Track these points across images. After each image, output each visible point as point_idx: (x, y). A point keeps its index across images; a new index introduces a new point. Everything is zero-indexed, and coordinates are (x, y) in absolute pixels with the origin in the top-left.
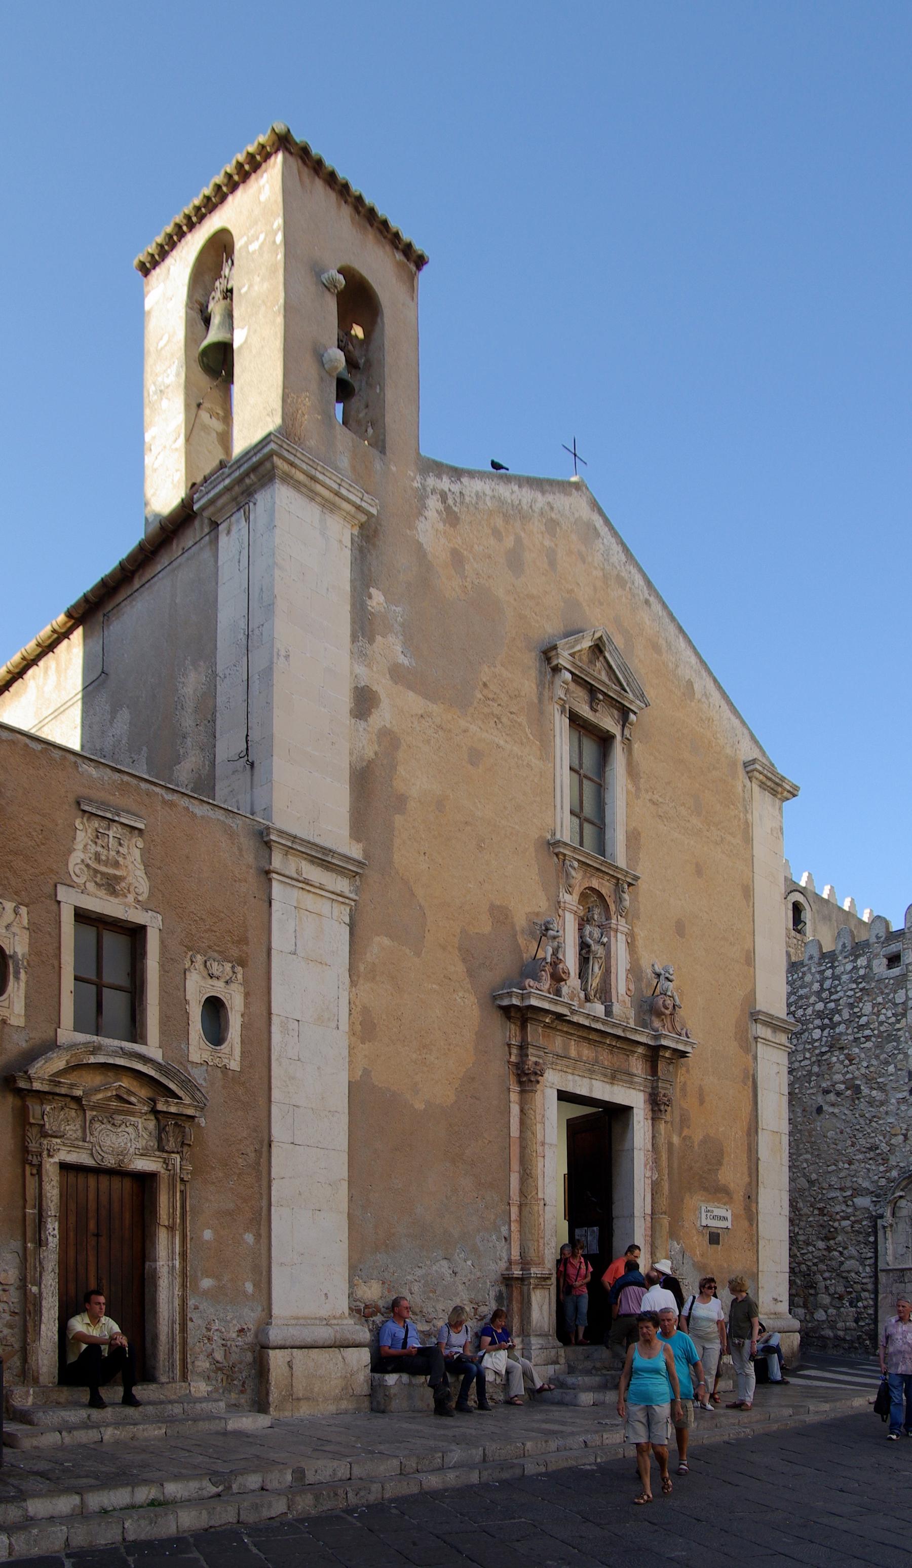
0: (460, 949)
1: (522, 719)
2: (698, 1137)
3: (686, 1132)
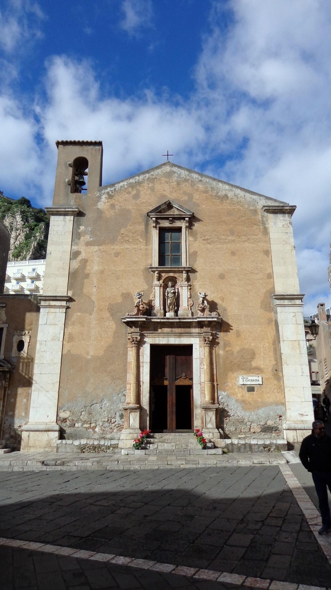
0: (108, 309)
1: (139, 237)
2: (236, 349)
3: (227, 349)
